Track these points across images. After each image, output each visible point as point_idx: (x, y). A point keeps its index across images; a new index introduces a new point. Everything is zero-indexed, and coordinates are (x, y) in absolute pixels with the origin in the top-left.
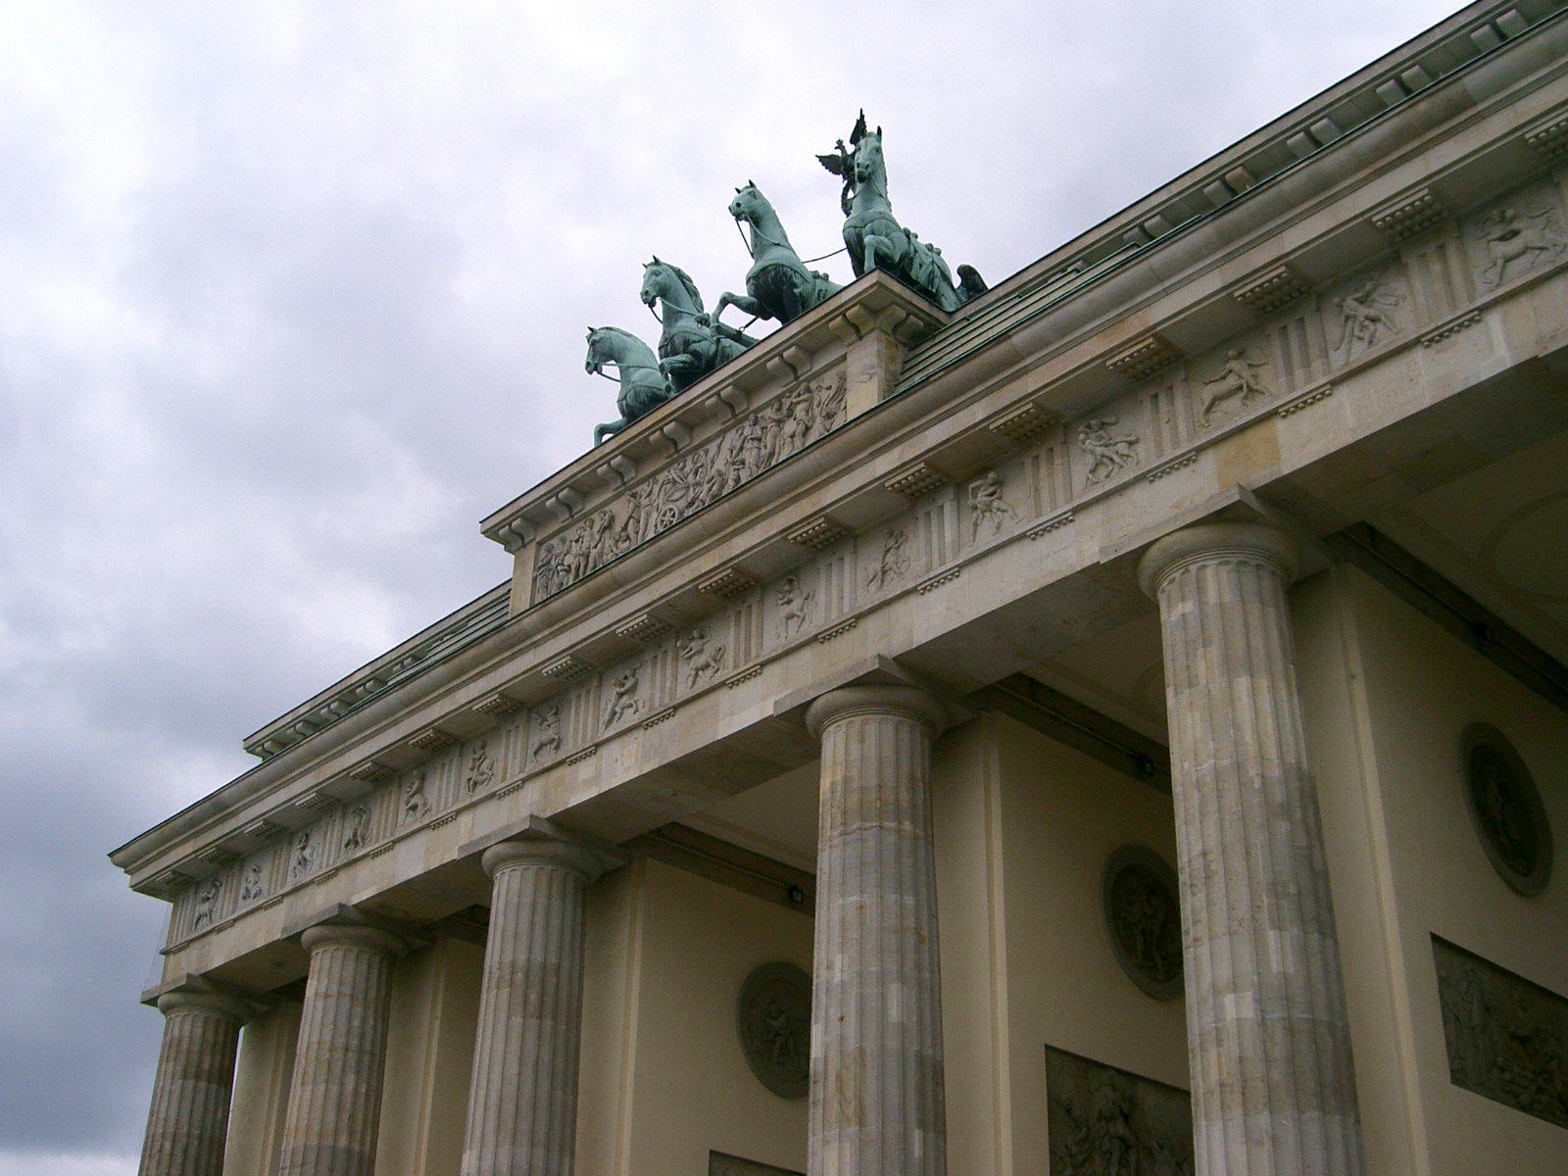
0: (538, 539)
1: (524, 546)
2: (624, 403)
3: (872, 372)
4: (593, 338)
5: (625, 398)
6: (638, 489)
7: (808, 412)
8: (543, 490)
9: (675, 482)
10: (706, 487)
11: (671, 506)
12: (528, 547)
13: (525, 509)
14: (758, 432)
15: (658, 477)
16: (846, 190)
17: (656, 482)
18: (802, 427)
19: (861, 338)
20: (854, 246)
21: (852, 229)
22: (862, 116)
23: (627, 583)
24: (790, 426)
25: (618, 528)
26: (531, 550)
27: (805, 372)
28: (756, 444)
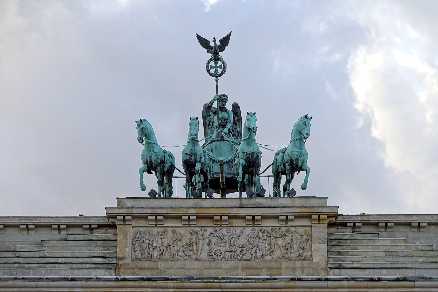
0: (133, 225)
1: (125, 225)
2: (149, 159)
3: (324, 241)
4: (141, 126)
5: (150, 157)
6: (196, 229)
7: (291, 240)
8: (149, 211)
9: (219, 236)
10: (239, 250)
11: (219, 248)
12: (127, 226)
13: (135, 214)
14: (265, 237)
15: (206, 228)
16: (211, 60)
17: (205, 230)
18: (289, 247)
19: (319, 223)
20: (294, 162)
21: (296, 156)
22: (230, 34)
23: (225, 288)
24: (280, 241)
25: (184, 242)
26: (128, 229)
27: (290, 223)
28: (264, 241)
